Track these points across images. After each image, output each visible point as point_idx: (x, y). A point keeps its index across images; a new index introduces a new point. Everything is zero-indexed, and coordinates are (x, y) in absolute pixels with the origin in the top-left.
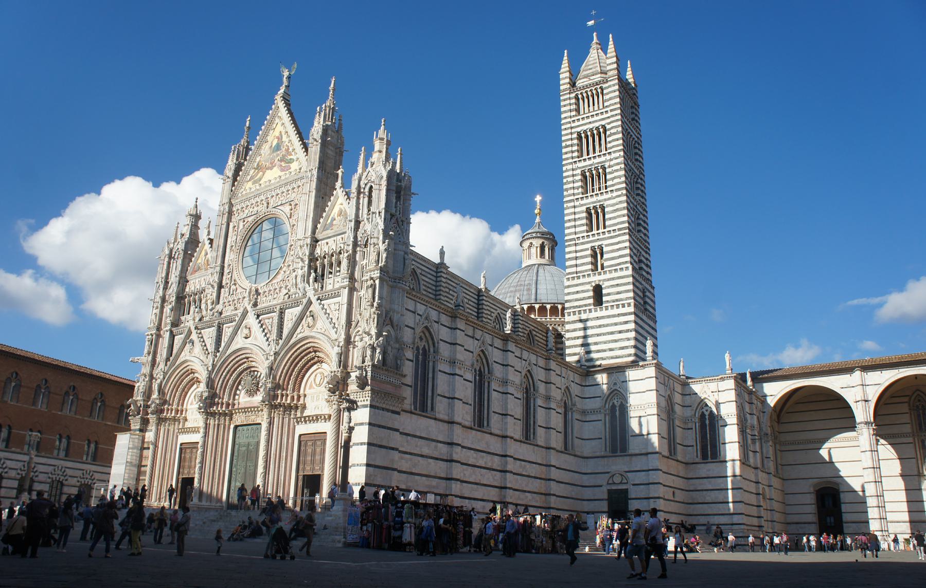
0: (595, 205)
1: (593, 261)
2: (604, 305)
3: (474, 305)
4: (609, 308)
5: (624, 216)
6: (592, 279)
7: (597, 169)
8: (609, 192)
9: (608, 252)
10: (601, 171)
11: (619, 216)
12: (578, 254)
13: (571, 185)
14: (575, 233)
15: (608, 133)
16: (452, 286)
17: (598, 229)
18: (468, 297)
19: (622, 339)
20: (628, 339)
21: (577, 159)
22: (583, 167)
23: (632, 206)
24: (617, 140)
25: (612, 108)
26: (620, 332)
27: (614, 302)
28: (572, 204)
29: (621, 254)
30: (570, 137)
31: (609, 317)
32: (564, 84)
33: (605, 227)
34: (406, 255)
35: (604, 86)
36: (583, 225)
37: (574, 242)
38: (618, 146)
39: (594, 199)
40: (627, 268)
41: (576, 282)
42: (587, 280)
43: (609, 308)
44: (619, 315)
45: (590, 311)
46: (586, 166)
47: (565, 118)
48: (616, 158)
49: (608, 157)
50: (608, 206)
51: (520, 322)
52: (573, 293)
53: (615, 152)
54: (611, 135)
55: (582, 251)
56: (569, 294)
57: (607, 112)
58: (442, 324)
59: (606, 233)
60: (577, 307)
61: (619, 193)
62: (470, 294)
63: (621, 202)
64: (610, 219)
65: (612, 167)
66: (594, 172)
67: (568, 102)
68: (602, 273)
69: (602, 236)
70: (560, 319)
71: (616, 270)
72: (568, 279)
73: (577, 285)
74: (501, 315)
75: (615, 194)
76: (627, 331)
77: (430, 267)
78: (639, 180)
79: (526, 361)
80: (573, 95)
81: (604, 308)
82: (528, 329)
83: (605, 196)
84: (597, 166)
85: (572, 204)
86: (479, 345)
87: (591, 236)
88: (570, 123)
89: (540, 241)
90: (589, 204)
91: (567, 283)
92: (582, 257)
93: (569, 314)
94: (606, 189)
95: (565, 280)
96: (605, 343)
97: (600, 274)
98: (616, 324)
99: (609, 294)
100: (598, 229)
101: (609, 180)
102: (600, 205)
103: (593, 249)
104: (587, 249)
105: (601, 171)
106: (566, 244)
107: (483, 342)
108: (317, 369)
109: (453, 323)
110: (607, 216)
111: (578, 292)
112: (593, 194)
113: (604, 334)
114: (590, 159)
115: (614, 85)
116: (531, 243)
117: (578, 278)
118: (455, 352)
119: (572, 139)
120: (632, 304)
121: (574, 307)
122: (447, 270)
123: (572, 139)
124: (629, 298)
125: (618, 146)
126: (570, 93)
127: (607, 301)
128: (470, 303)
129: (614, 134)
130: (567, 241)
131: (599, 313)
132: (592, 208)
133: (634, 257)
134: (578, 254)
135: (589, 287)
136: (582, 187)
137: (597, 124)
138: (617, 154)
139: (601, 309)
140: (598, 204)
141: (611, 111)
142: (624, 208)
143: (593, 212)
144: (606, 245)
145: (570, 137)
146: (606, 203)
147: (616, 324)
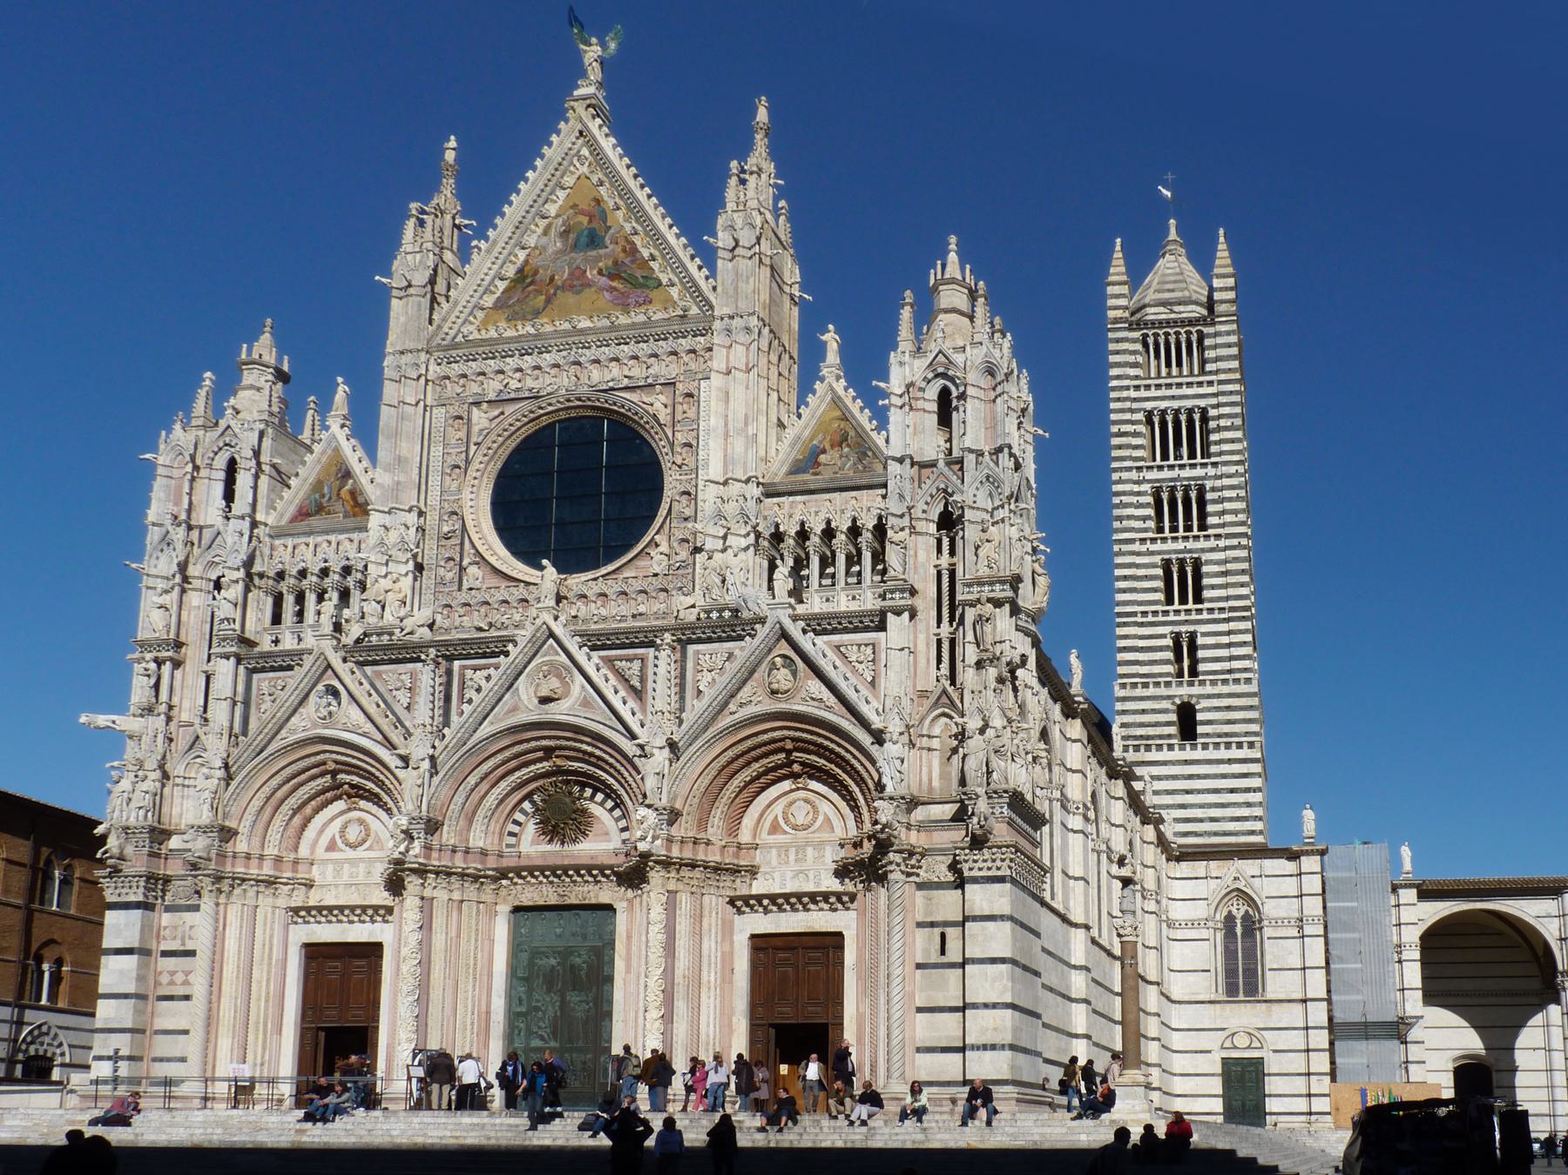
0: (1181, 556)
9: (1206, 647)
15: (1212, 424)
21: (1141, 464)
24: (1233, 441)
36: (1155, 590)
38: (1232, 453)
39: (1180, 545)
40: (1248, 681)
41: (1139, 692)
42: (1163, 691)
49: (1211, 471)
50: (1209, 562)
54: (1219, 429)
59: (1205, 612)
64: (1213, 587)
65: (1222, 489)
66: (1179, 495)
69: (1194, 617)
72: (1123, 686)
83: (1202, 544)
90: (1169, 552)
91: (1120, 693)
97: (1191, 684)
104: (1163, 636)
105: (1193, 495)
108: (792, 791)
110: (1205, 581)
114: (1171, 467)
117: (1146, 685)
125: (1232, 453)
129: (1226, 429)
130: (1120, 615)
138: (1232, 469)
141: (1220, 382)
143: (1175, 569)
146: (1204, 557)
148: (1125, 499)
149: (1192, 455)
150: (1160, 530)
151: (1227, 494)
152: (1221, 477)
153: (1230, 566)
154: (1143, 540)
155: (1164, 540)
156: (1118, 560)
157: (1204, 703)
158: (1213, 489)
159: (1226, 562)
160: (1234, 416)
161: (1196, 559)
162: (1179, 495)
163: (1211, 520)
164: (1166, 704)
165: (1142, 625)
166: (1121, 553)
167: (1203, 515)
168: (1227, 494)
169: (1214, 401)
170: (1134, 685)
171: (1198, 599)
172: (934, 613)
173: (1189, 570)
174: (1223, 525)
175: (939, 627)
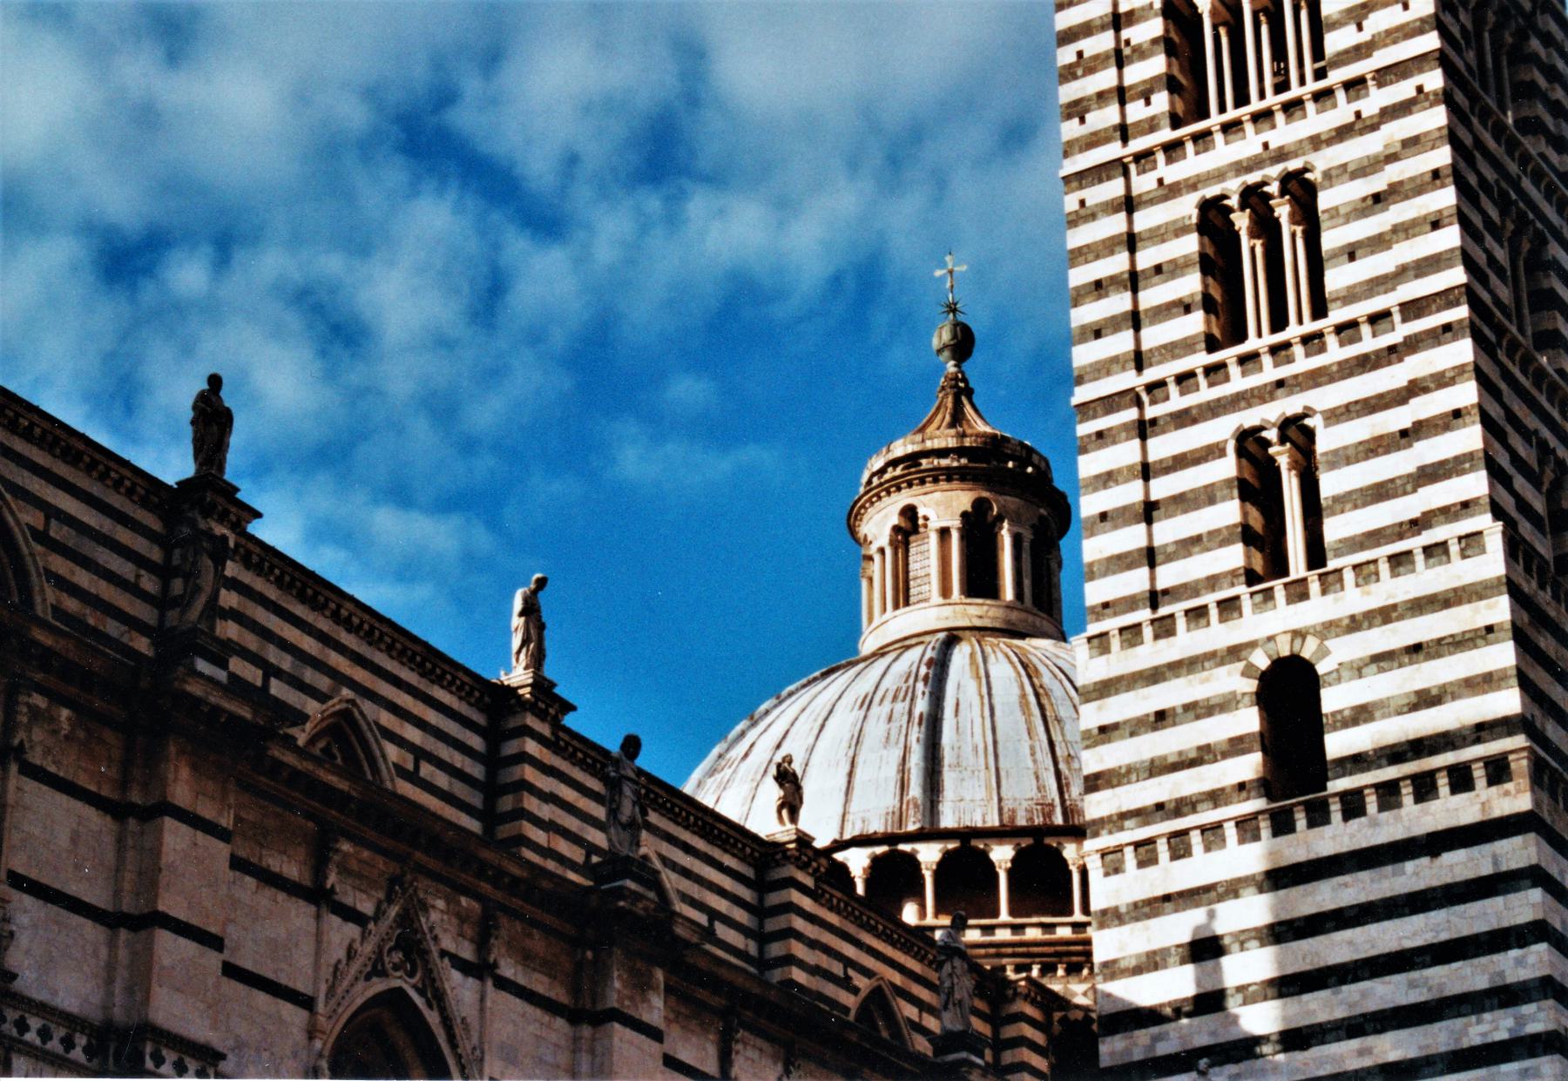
0: (1253, 178)
1: (1256, 520)
3: (460, 790)
4: (1372, 802)
5: (1436, 225)
8: (1341, 95)
11: (1405, 230)
12: (1162, 488)
13: (1106, 79)
16: (285, 645)
17: (1279, 323)
18: (413, 734)
23: (1490, 175)
28: (1114, 188)
33: (1319, 310)
37: (1131, 414)
41: (1151, 653)
42: (1218, 635)
43: (1372, 802)
51: (799, 924)
55: (1181, 462)
56: (1106, 732)
59: (1331, 341)
61: (1403, 90)
62: (432, 717)
63: (1413, 144)
68: (1314, 587)
69: (1302, 363)
70: (1079, 927)
71: (1399, 562)
73: (1154, 676)
74: (671, 880)
75: (1374, 101)
77: (116, 500)
78: (1535, 44)
81: (1335, 808)
82: (861, 982)
83: (1316, 121)
85: (1114, 188)
86: (368, 948)
87: (1234, 370)
89: (962, 499)
90: (1219, 175)
92: (1183, 502)
93: (1112, 861)
94: (1320, 74)
97: (1298, 592)
99: (1361, 714)
101: (1336, 25)
104: (1213, 452)
106: (1085, 429)
110: (1331, 239)
111: (1161, 718)
112: (1244, 111)
116: (909, 512)
117: (1165, 628)
118: (142, 976)
120: (1520, 765)
121: (1143, 815)
122: (239, 528)
124: (1504, 726)
128: (426, 770)
132: (1233, 202)
133: (1520, 482)
134: (1162, 488)
135: (1233, 681)
136: (1171, 84)
139: (1318, 816)
140: (1274, 171)
142: (1436, 174)
143: (1241, 221)
144: (1336, 416)
146: (1322, 161)
154: (1144, 157)
156: (1079, 237)
163: (1335, 42)
166: (1085, 215)
170: (1132, 634)
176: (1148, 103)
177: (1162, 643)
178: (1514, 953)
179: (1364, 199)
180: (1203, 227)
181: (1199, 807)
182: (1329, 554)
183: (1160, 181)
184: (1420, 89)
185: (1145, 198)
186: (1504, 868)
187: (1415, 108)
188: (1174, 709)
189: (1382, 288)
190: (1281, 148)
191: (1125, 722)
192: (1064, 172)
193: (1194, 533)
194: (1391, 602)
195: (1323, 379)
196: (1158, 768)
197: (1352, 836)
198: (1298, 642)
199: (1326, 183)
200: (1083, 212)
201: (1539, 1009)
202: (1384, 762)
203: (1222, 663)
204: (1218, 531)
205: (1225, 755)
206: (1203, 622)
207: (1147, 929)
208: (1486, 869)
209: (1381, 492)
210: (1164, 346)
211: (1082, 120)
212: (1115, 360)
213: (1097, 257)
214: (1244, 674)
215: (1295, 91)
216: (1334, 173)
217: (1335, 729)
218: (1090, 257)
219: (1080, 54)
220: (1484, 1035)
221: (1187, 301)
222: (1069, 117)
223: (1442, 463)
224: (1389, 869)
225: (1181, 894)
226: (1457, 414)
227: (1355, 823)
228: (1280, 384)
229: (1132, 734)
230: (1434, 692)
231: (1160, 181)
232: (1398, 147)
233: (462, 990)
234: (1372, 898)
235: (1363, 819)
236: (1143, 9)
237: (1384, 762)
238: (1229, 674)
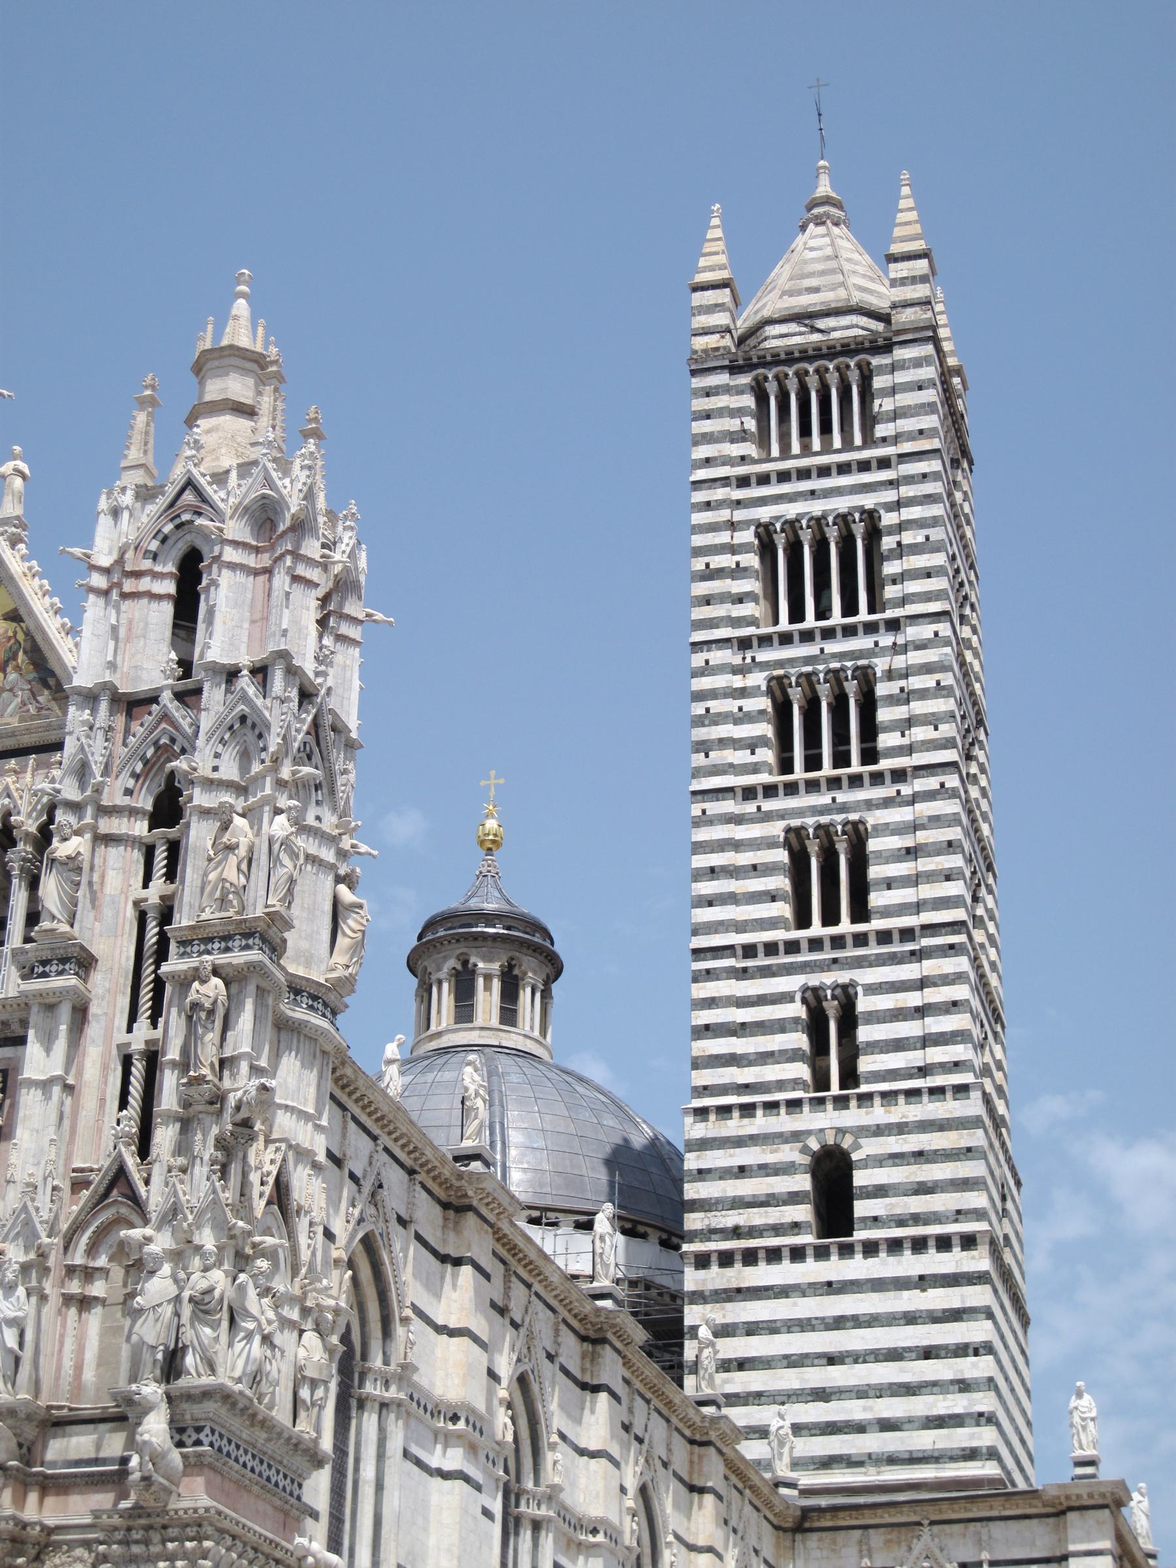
0: (824, 820)
2: (860, 1235)
6: (808, 1120)
7: (836, 676)
10: (851, 687)
14: (740, 927)
15: (888, 543)
17: (830, 917)
19: (934, 1384)
20: (964, 1386)
22: (780, 664)
25: (907, 447)
26: (928, 1353)
27: (901, 1222)
29: (935, 1029)
30: (724, 537)
31: (878, 1285)
32: (706, 332)
34: (343, 889)
35: (876, 361)
38: (928, 597)
40: (961, 1090)
41: (735, 1126)
42: (784, 1122)
44: (923, 1282)
45: (798, 1254)
46: (791, 662)
47: (708, 462)
48: (921, 646)
49: (886, 640)
52: (726, 1174)
53: (914, 618)
54: (901, 550)
56: (702, 1174)
57: (884, 463)
58: (419, 1238)
60: (736, 1232)
63: (936, 821)
64: (889, 884)
66: (824, 692)
67: (722, 401)
73: (739, 1142)
76: (962, 1350)
79: (640, 1441)
80: (745, 379)
81: (859, 1248)
84: (835, 665)
88: (725, 481)
91: (698, 1130)
93: (702, 1261)
95: (689, 1120)
96: (861, 1393)
97: (841, 1102)
98: (910, 1318)
99: (880, 1191)
100: (830, 917)
102: (846, 823)
103: (813, 999)
104: (785, 998)
105: (851, 687)
107: (530, 1336)
109: (452, 1236)
110: (875, 872)
111: (742, 1171)
113: (858, 1358)
114: (807, 636)
115: (918, 363)
117: (748, 1110)
119: (733, 549)
123: (733, 549)
125: (928, 597)
126: (734, 369)
127: (875, 1219)
129: (916, 549)
131: (836, 1269)
137: (842, 504)
138: (925, 631)
139: (846, 1251)
141: (903, 457)
142: (950, 844)
143: (813, 847)
144: (872, 989)
145: (724, 537)
146: (873, 818)
147: (910, 1318)
148: (716, 706)
149: (850, 608)
150: (786, 766)
151: (916, 682)
152: (904, 649)
153: (923, 836)
154: (749, 793)
155: (791, 789)
157: (871, 1147)
158: (890, 675)
159: (915, 827)
160: (934, 522)
161: (855, 824)
162: (824, 692)
163: (886, 740)
164: (789, 1153)
165: (743, 974)
167: (869, 730)
168: (916, 682)
169: (890, 496)
170: (724, 1111)
171: (861, 912)
172: (124, 1002)
173: (842, 847)
174: (910, 750)
175: (130, 1030)
176: (753, 753)
177: (746, 1121)
178: (972, 1359)
179: (900, 849)
180: (787, 844)
181: (765, 1234)
182: (862, 1080)
183: (759, 808)
184: (942, 785)
185: (747, 817)
186: (968, 1305)
187: (938, 797)
188: (751, 1166)
189: (908, 911)
190: (845, 803)
191: (716, 1169)
192: (692, 788)
193: (769, 1049)
194: (904, 1120)
195: (865, 964)
196: (739, 1203)
197: (868, 1269)
198: (840, 1135)
199: (874, 834)
200: (704, 818)
201: (985, 1397)
202: (893, 1224)
203: (786, 1142)
204: (786, 1051)
205: (785, 1203)
206: (775, 1111)
207: (723, 1309)
208: (957, 1304)
209: (898, 1045)
210: (756, 920)
211: (707, 756)
212: (721, 923)
213: (712, 852)
214: (801, 1152)
215: (856, 767)
216: (880, 828)
217: (862, 1198)
218: (707, 849)
219: (708, 710)
220: (948, 1407)
221: (774, 893)
222: (697, 751)
223: (942, 1034)
224: (892, 1293)
225: (748, 1289)
226: (955, 1004)
227: (871, 1261)
228: (835, 961)
229: (721, 1178)
230: (930, 1185)
231: (759, 808)
232: (925, 821)
233: (547, 1368)
234: (879, 1311)
235: (876, 1259)
236: (753, 687)
237: (893, 1224)
238: (791, 1150)
